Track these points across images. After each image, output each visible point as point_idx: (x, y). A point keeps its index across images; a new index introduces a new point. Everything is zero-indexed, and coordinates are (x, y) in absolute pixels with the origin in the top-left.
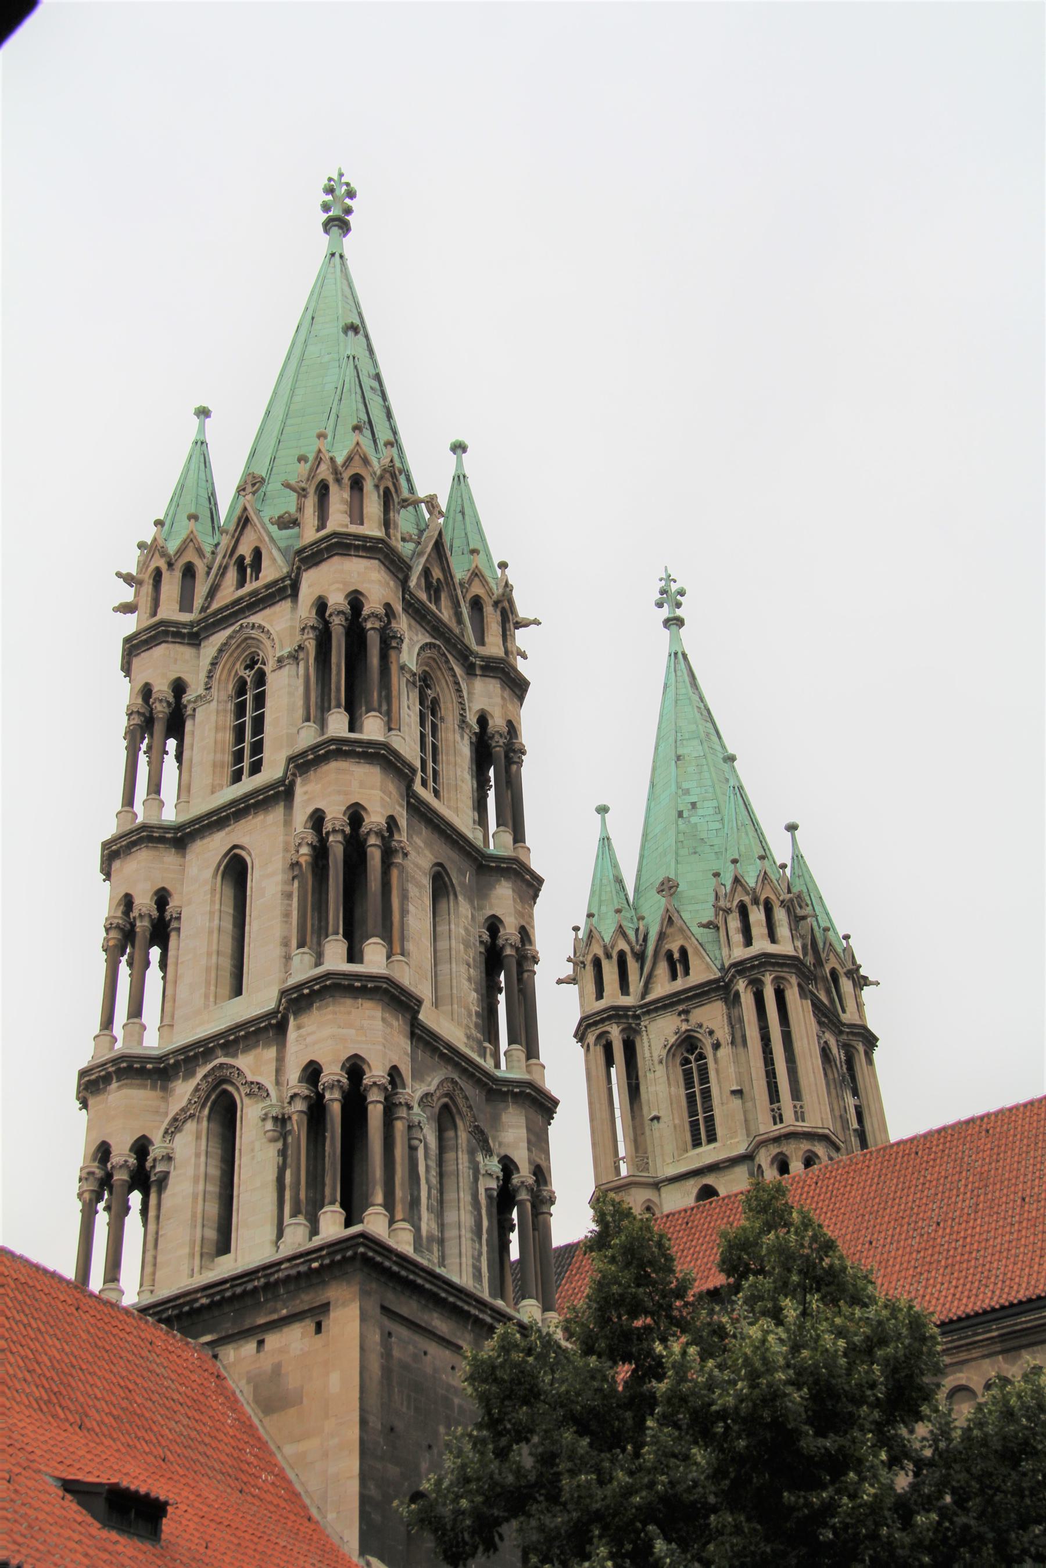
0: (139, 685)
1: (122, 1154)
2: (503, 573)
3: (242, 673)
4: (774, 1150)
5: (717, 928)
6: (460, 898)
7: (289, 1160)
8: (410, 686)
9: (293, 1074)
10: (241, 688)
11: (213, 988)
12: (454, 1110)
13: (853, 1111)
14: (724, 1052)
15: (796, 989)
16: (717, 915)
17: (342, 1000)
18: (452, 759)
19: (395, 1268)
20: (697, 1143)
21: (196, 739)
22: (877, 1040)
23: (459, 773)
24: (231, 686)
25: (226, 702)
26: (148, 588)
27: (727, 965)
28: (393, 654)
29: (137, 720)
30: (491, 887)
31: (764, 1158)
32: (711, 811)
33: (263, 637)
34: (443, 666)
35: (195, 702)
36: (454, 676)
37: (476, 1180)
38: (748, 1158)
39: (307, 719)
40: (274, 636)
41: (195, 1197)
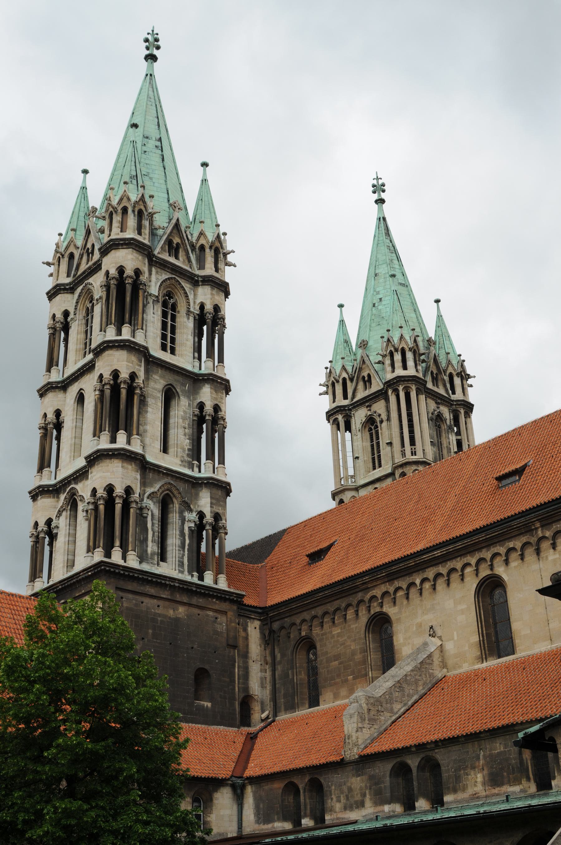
5: (383, 363)
6: (181, 398)
11: (73, 453)
12: (172, 495)
13: (455, 443)
14: (384, 424)
15: (415, 392)
17: (105, 460)
19: (122, 572)
22: (473, 405)
30: (200, 388)
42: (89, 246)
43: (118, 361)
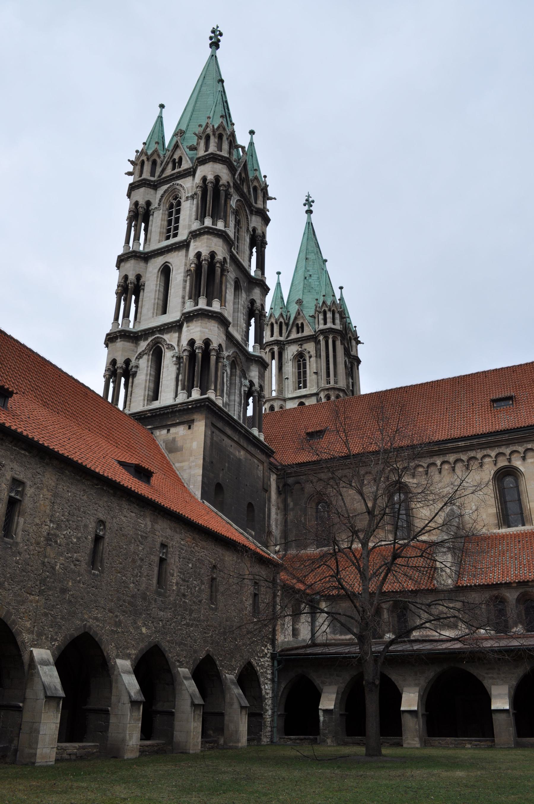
0: (134, 201)
1: (120, 363)
2: (265, 179)
4: (326, 393)
5: (315, 318)
6: (243, 291)
7: (181, 372)
8: (232, 213)
9: (184, 343)
10: (171, 206)
11: (155, 311)
13: (351, 383)
14: (313, 359)
15: (339, 341)
16: (315, 313)
17: (204, 319)
18: (243, 242)
20: (300, 388)
21: (154, 223)
22: (361, 362)
23: (245, 247)
24: (167, 206)
25: (166, 211)
26: (138, 167)
27: (317, 330)
28: (228, 200)
29: (132, 214)
30: (253, 289)
31: (322, 395)
32: (316, 278)
33: (181, 189)
34: (243, 209)
35: (154, 209)
36: (246, 213)
37: (241, 387)
38: (317, 394)
39: (197, 219)
40: (186, 189)
41: (146, 381)
43: (216, 245)
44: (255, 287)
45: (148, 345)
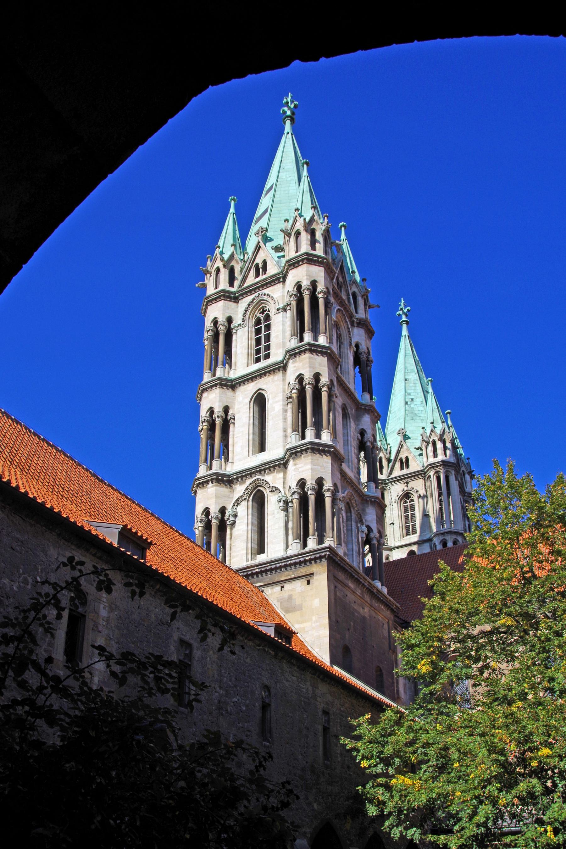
3: (259, 315)
10: (258, 322)
24: (254, 321)
33: (269, 299)
35: (238, 327)
40: (275, 299)
42: (259, 260)
44: (364, 414)
45: (247, 489)
